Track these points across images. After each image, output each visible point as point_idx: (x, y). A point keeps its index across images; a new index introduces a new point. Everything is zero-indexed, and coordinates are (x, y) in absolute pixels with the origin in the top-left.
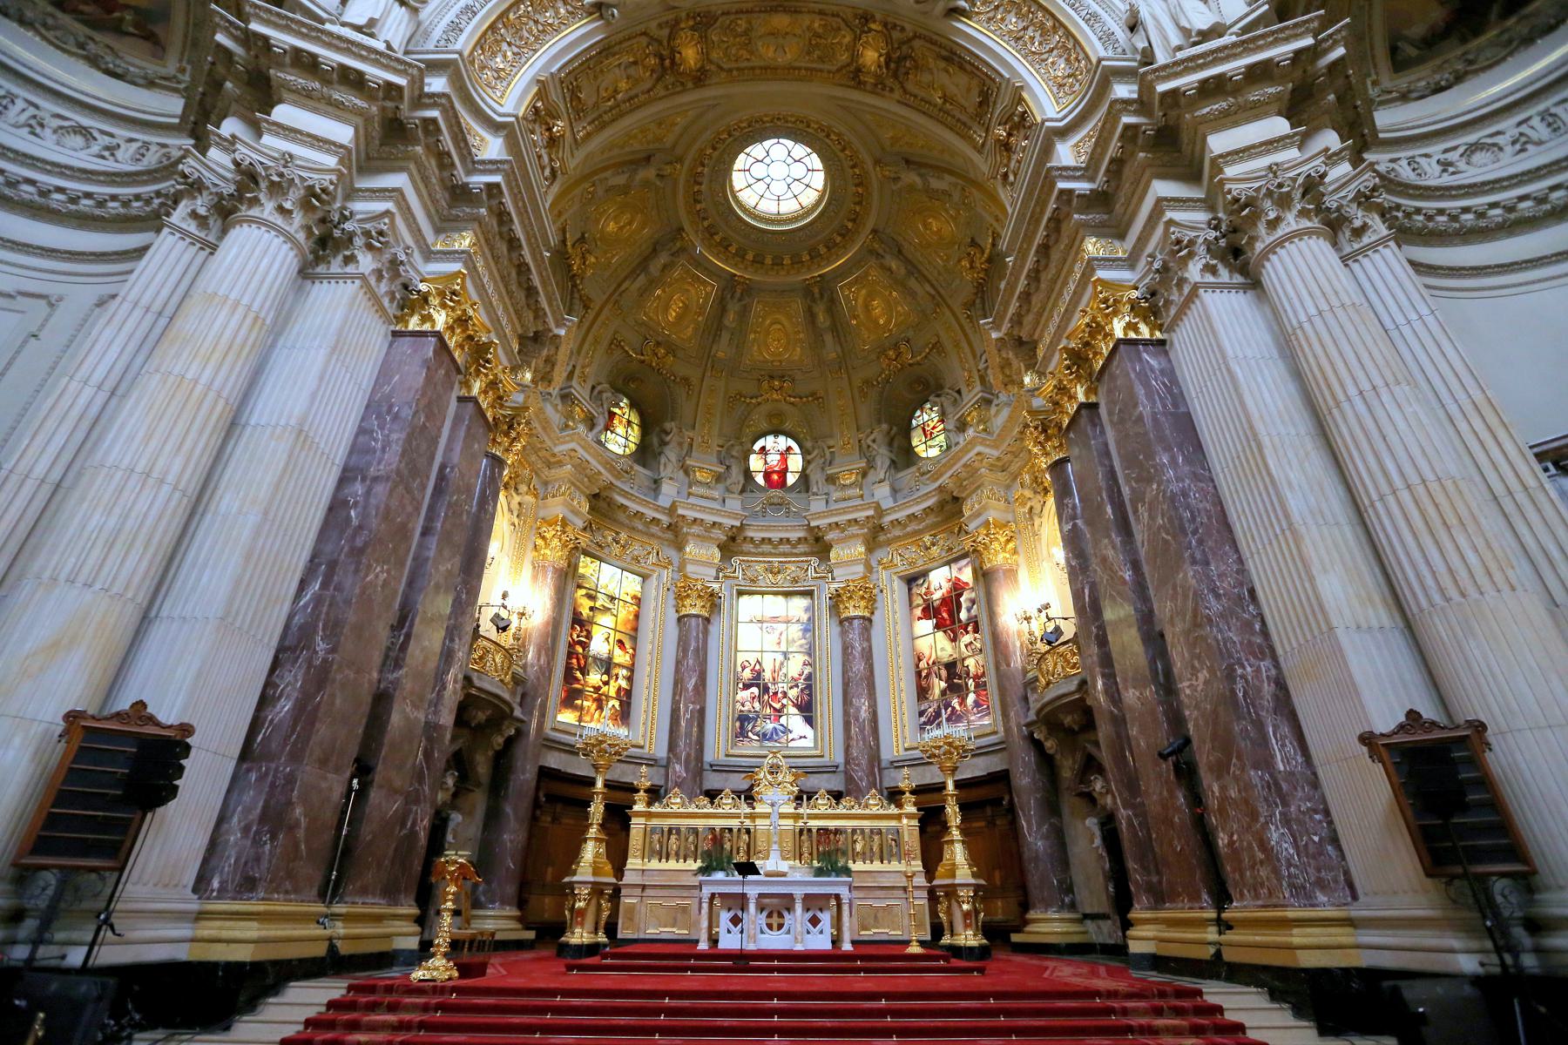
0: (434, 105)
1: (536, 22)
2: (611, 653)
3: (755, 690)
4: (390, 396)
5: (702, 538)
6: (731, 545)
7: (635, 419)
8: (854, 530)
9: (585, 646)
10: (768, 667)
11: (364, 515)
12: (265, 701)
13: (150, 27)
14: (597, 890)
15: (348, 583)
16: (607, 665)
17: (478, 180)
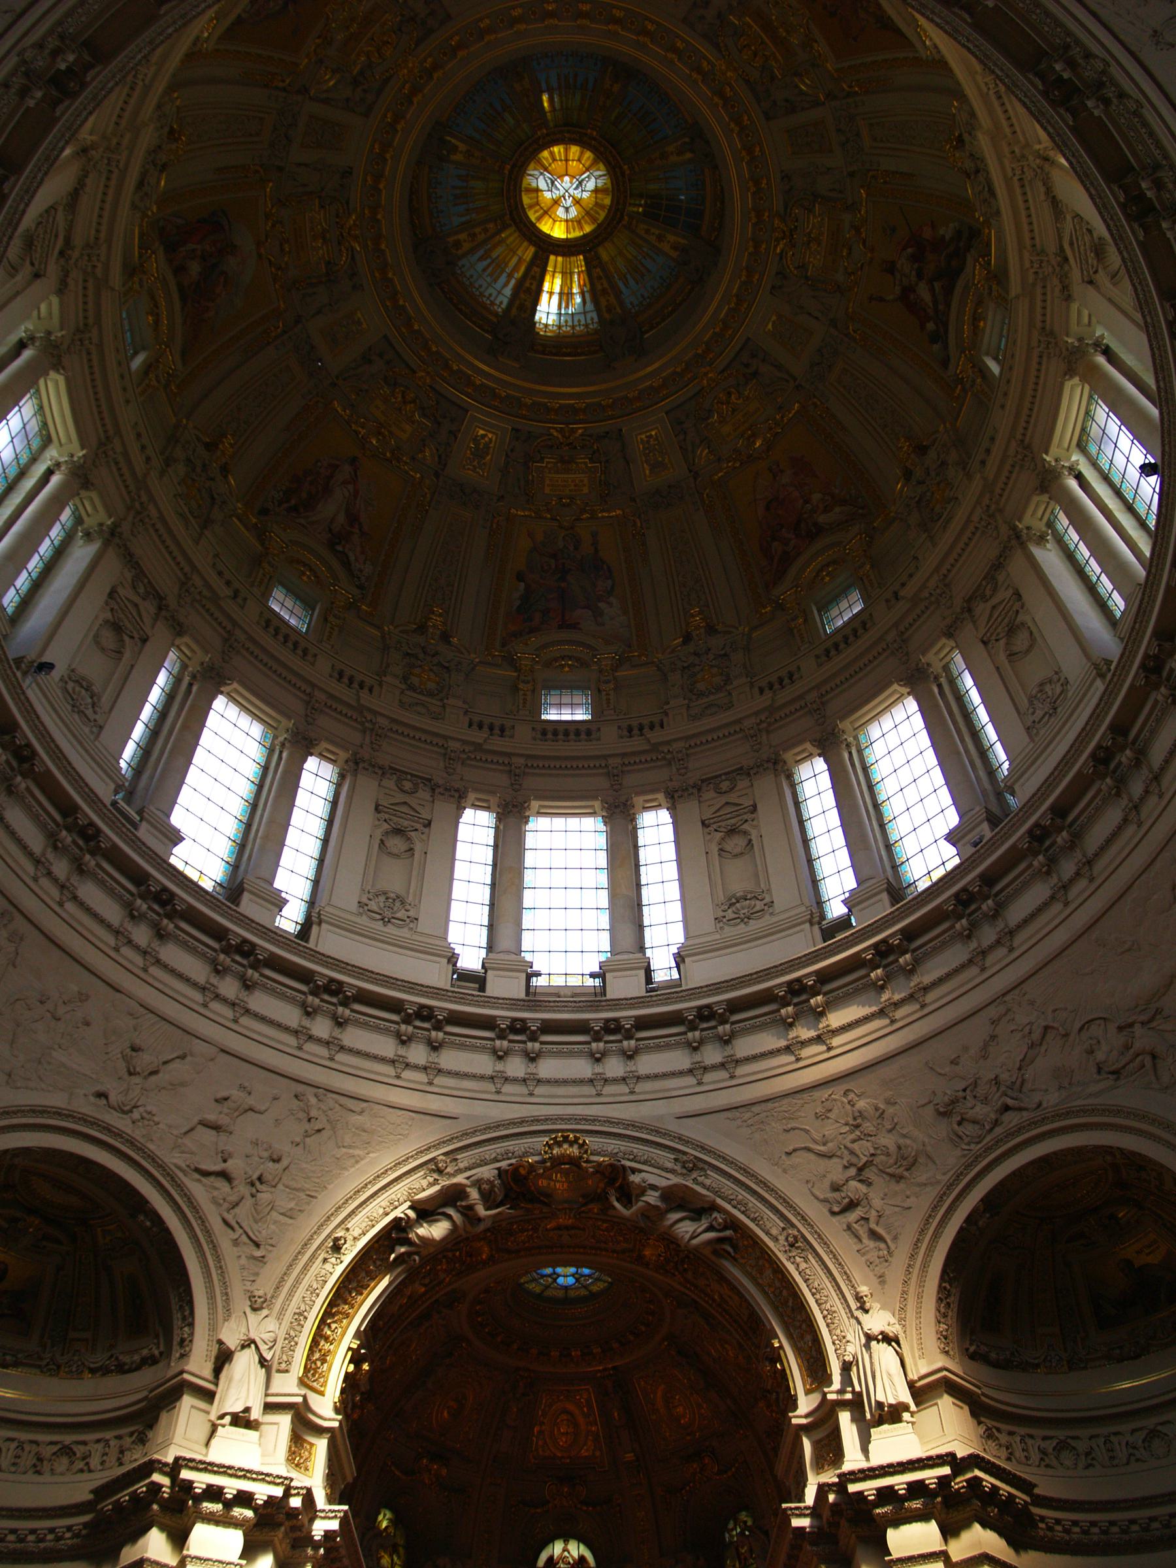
0: (298, 1494)
7: (401, 1541)
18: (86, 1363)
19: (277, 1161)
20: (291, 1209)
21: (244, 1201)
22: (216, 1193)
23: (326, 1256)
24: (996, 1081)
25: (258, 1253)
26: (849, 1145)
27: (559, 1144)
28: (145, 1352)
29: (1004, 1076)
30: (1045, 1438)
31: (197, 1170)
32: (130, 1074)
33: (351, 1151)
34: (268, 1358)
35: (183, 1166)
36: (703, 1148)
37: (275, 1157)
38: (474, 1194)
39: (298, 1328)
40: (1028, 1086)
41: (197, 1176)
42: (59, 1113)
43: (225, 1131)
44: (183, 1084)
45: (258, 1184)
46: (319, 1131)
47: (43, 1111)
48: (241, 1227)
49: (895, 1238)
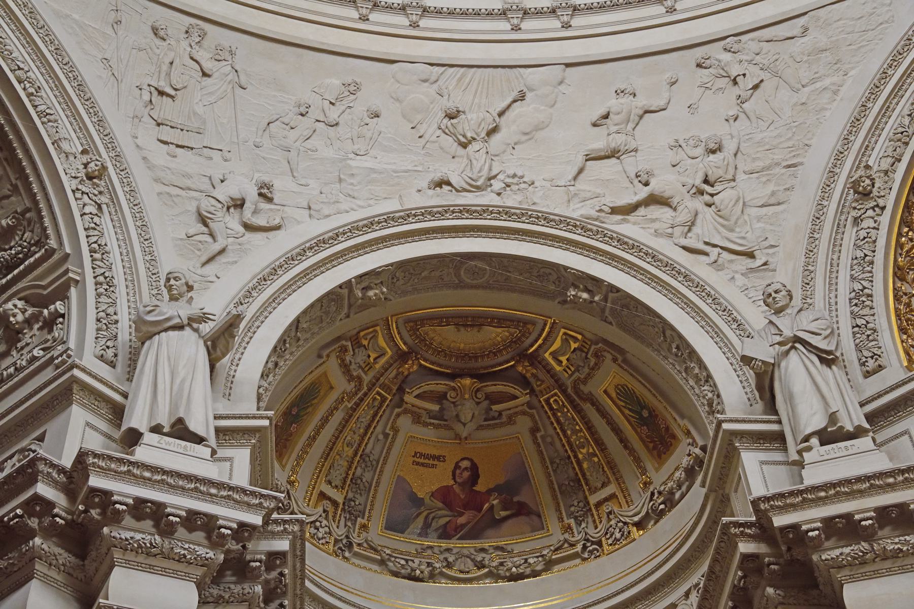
13: (515, 499)
18: (628, 520)
20: (773, 193)
21: (700, 216)
22: (657, 225)
23: (854, 213)
28: (685, 461)
31: (614, 211)
32: (464, 146)
33: (818, 85)
34: (832, 347)
37: (712, 146)
39: (866, 311)
42: (389, 219)
43: (627, 152)
44: (538, 128)
46: (756, 87)
47: (370, 224)
48: (715, 246)
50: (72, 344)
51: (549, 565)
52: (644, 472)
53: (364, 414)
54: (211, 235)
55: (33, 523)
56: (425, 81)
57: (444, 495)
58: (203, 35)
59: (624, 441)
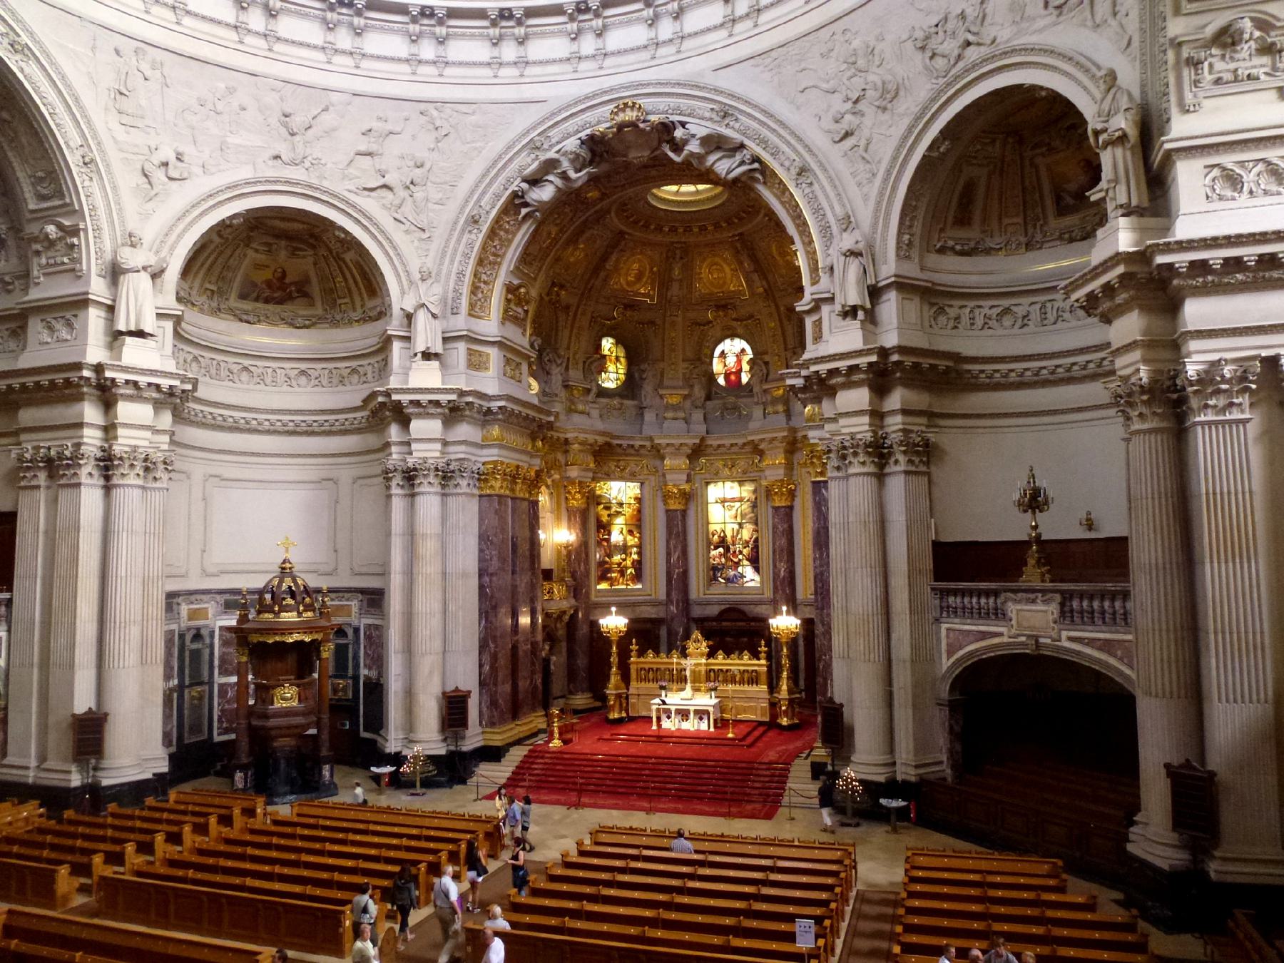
1: (495, 247)
2: (625, 539)
3: (721, 550)
4: (486, 531)
5: (676, 455)
6: (696, 453)
7: (622, 353)
8: (776, 443)
9: (608, 540)
10: (729, 534)
11: (492, 591)
12: (481, 666)
14: (619, 696)
15: (494, 620)
16: (625, 549)
17: (495, 405)
19: (422, 166)
22: (384, 201)
23: (470, 228)
24: (962, 16)
25: (425, 236)
26: (846, 82)
27: (623, 110)
29: (971, 12)
30: (993, 307)
31: (365, 189)
32: (293, 135)
35: (353, 188)
36: (732, 96)
37: (419, 164)
38: (566, 165)
40: (988, 20)
41: (366, 193)
44: (334, 130)
45: (411, 186)
49: (879, 162)
50: (84, 268)
51: (316, 323)
52: (362, 299)
53: (229, 252)
54: (150, 183)
55: (82, 383)
56: (273, 90)
57: (269, 284)
58: (145, 53)
59: (356, 282)
